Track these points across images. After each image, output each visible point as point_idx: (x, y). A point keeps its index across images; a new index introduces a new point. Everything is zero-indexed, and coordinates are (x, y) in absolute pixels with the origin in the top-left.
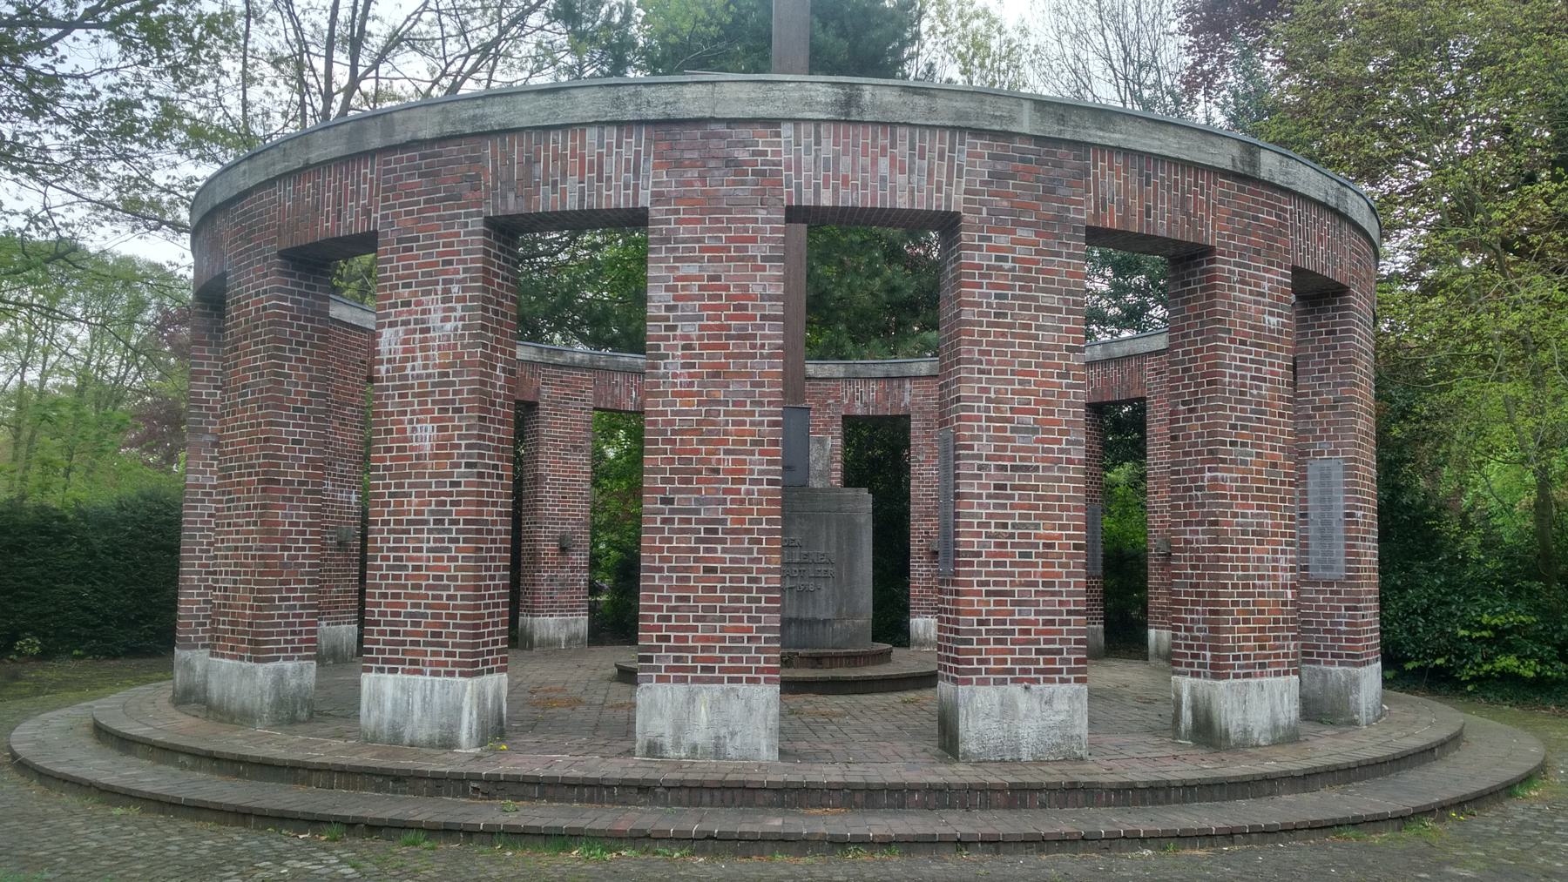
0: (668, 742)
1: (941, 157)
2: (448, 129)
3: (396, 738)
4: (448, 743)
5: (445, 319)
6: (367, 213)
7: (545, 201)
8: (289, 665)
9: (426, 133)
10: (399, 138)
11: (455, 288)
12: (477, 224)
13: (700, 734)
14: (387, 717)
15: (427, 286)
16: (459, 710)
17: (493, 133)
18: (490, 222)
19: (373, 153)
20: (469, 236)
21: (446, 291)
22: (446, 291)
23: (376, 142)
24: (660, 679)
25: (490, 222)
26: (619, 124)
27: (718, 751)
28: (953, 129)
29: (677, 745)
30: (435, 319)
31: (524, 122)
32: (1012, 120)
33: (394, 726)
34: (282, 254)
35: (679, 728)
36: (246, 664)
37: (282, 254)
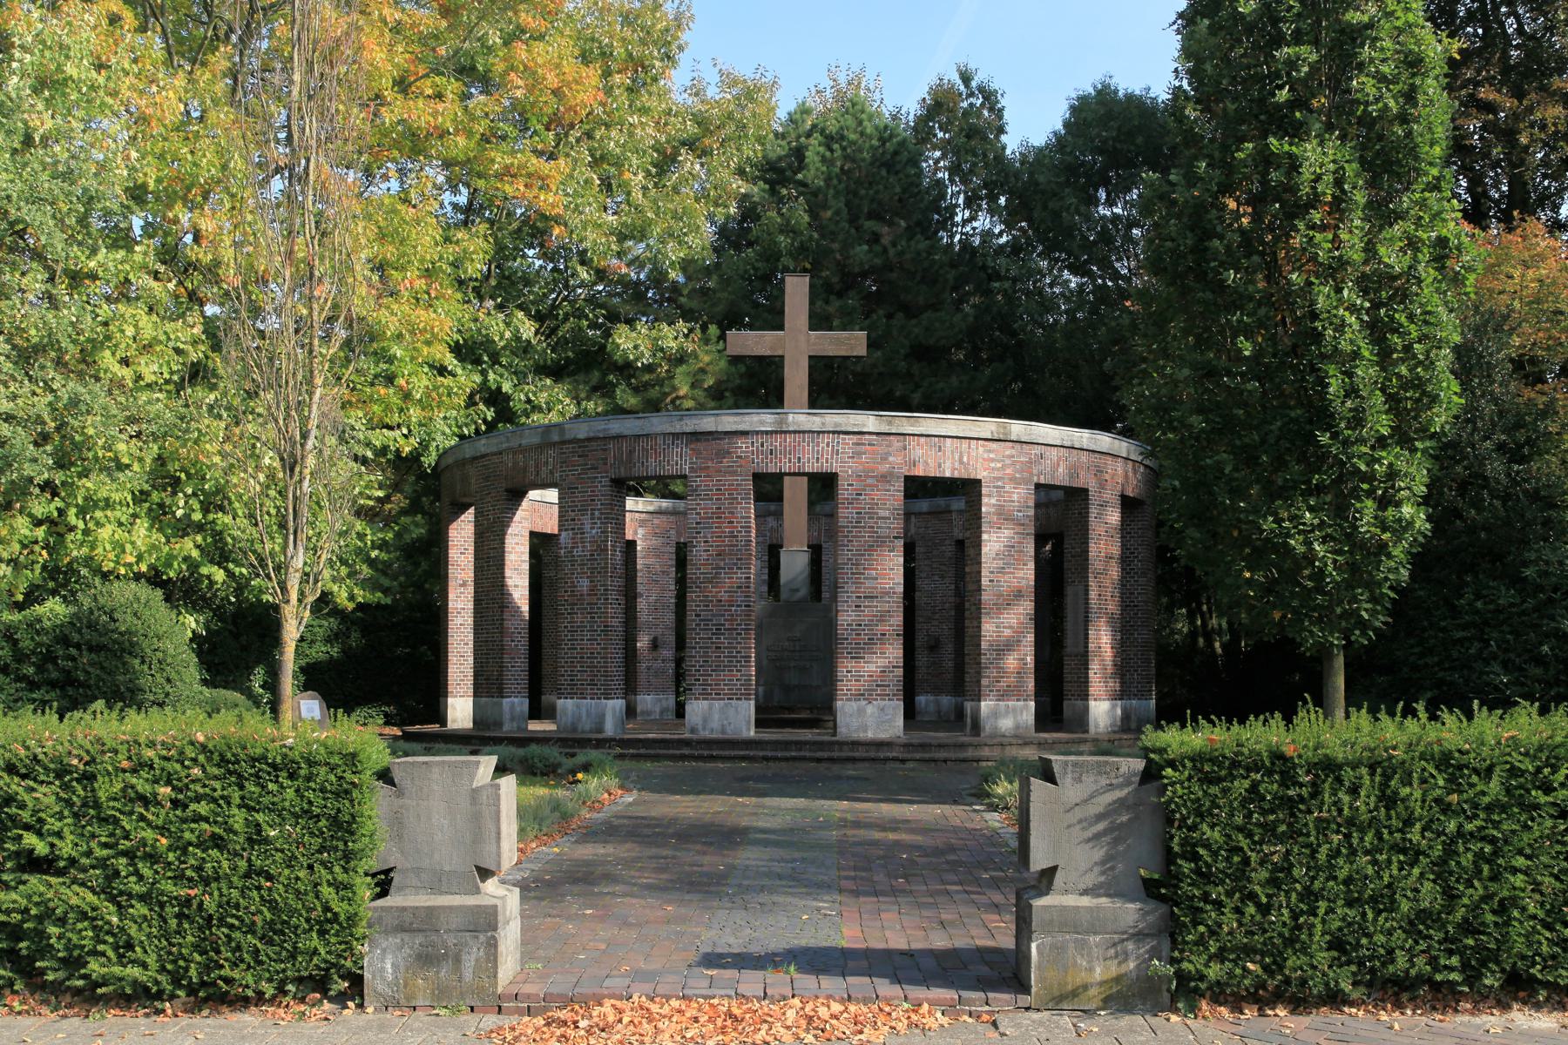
0: (700, 727)
1: (828, 445)
2: (592, 435)
3: (574, 730)
4: (600, 730)
5: (592, 528)
6: (552, 472)
7: (639, 471)
8: (516, 700)
9: (581, 436)
10: (568, 437)
11: (597, 513)
12: (605, 481)
13: (715, 723)
14: (570, 720)
15: (583, 511)
16: (604, 715)
17: (614, 438)
18: (612, 480)
19: (554, 444)
20: (602, 485)
21: (592, 514)
22: (592, 514)
23: (556, 438)
24: (696, 699)
25: (612, 480)
26: (673, 434)
27: (723, 732)
28: (834, 432)
29: (704, 729)
30: (587, 527)
31: (626, 432)
32: (864, 425)
33: (573, 723)
34: (507, 490)
35: (705, 720)
36: (495, 700)
37: (507, 490)
